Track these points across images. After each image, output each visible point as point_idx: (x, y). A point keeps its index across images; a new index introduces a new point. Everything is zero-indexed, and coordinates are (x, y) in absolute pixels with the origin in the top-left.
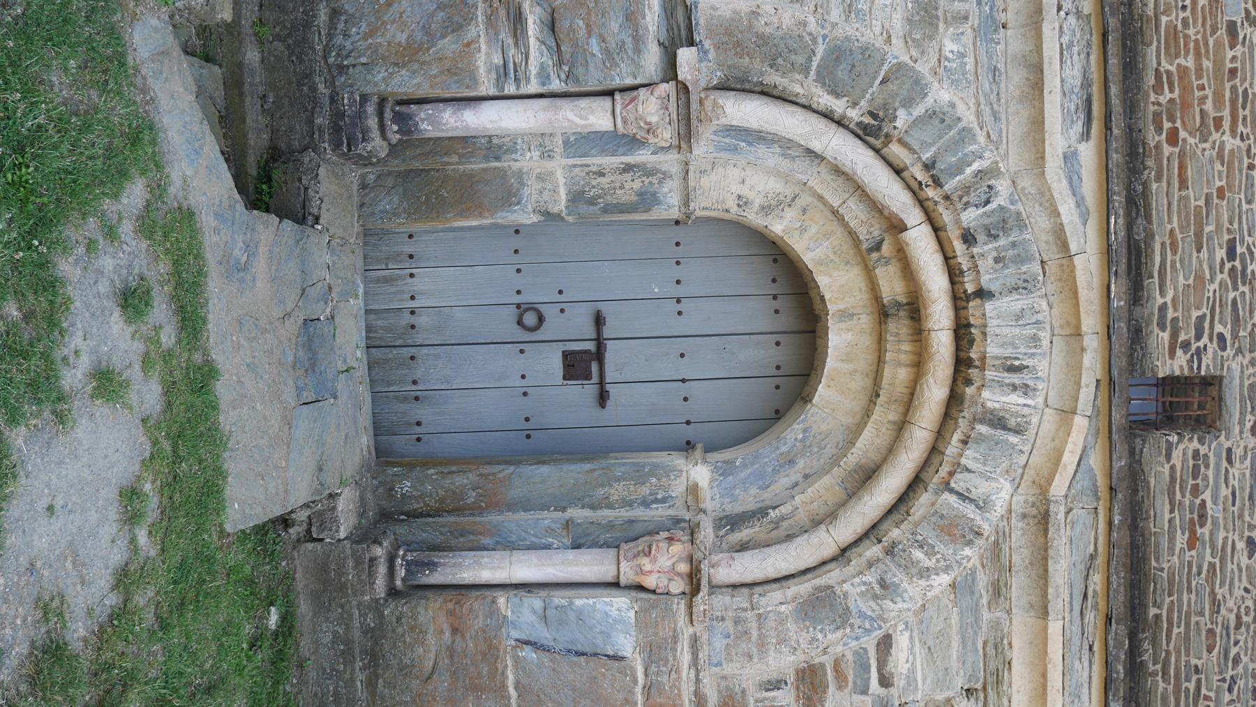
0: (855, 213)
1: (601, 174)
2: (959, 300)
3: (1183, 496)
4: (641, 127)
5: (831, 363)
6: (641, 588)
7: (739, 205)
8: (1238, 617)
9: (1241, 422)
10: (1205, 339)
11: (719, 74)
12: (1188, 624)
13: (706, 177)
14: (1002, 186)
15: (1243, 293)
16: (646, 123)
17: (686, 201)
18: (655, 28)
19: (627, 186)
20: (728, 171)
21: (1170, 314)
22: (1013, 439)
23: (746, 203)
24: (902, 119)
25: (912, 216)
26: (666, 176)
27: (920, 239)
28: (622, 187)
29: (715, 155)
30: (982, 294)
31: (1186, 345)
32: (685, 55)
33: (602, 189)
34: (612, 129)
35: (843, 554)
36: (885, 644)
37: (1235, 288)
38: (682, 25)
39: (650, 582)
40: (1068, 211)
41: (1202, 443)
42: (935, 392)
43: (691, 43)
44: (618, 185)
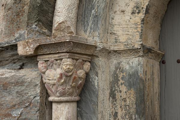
1: (116, 115)
4: (65, 82)
7: (138, 13)
11: (34, 26)
13: (120, 38)
16: (61, 78)
17: (133, 51)
18: (13, 71)
19: (124, 96)
20: (116, 23)
23: (137, 8)
26: (118, 67)
28: (125, 100)
29: (101, 31)
33: (125, 115)
34: (75, 105)
38: (11, 53)
43: (14, 47)
44: (123, 103)
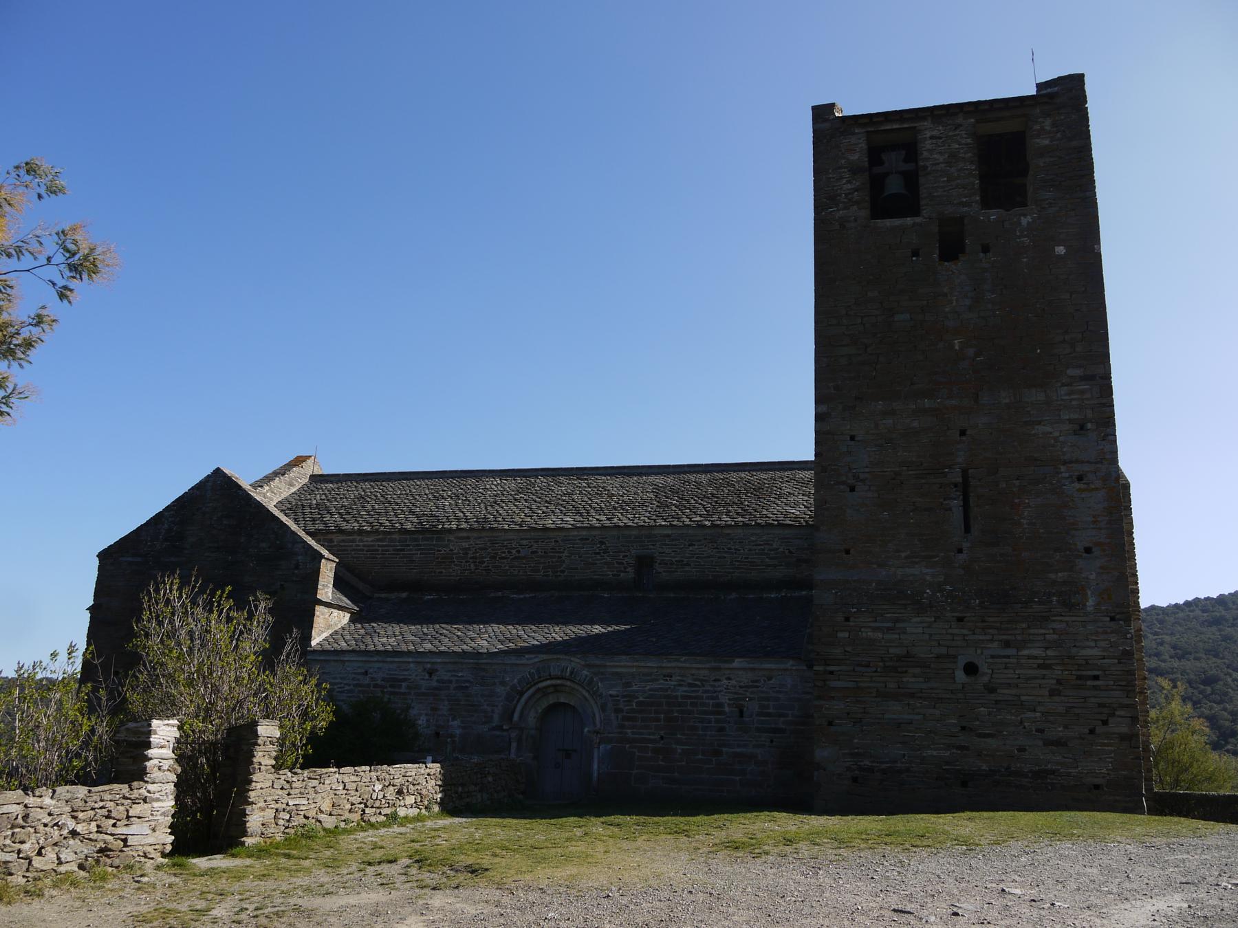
2: (552, 679)
3: (673, 568)
5: (567, 702)
6: (599, 743)
8: (714, 549)
9: (651, 549)
10: (624, 561)
12: (715, 566)
14: (532, 671)
15: (611, 550)
21: (615, 573)
22: (575, 670)
24: (519, 688)
25: (537, 686)
27: (541, 685)
30: (550, 675)
31: (625, 568)
32: (505, 727)
35: (596, 703)
36: (611, 696)
37: (609, 552)
39: (598, 741)
40: (536, 660)
41: (656, 562)
42: (568, 683)
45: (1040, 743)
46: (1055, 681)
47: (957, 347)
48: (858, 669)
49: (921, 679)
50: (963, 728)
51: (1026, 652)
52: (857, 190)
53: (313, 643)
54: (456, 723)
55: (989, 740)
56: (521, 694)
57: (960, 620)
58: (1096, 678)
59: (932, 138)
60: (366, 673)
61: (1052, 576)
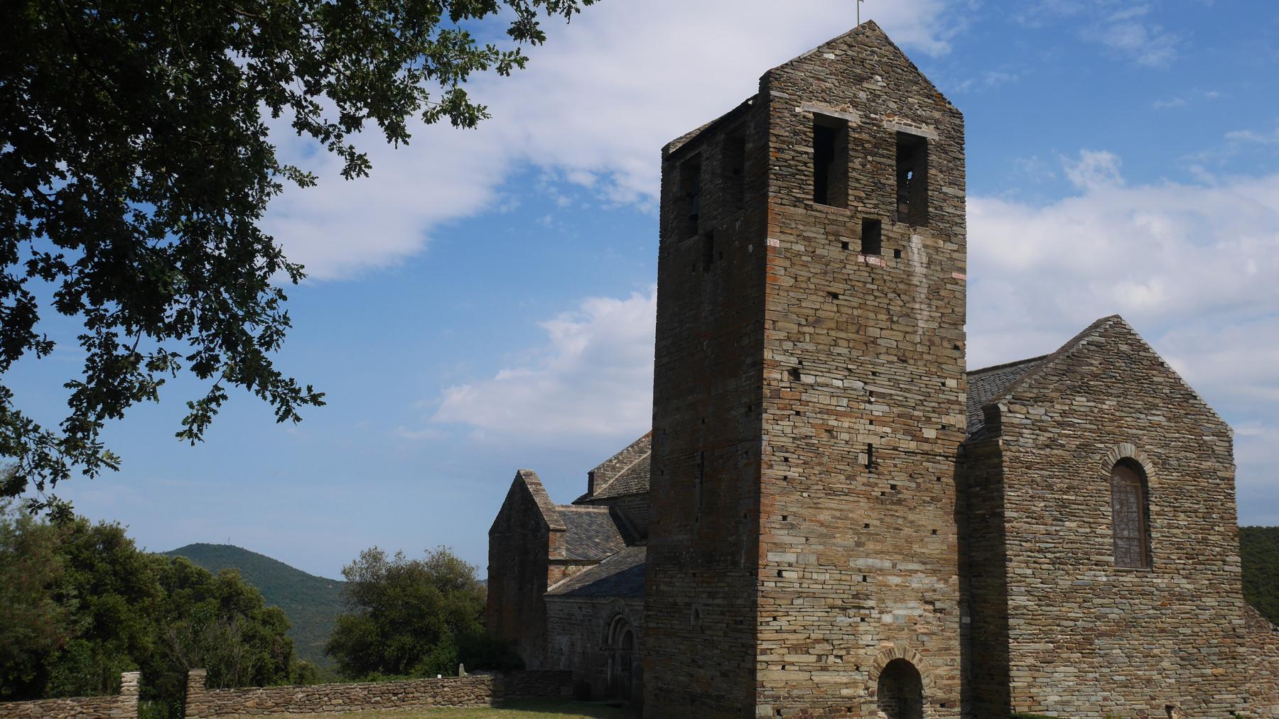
0: (619, 626)
45: (718, 674)
46: (725, 625)
47: (705, 348)
48: (659, 614)
49: (678, 622)
50: (693, 661)
51: (716, 601)
52: (675, 219)
53: (549, 589)
54: (589, 645)
55: (701, 671)
56: (609, 625)
57: (694, 575)
58: (741, 622)
59: (707, 159)
60: (562, 610)
61: (730, 539)
